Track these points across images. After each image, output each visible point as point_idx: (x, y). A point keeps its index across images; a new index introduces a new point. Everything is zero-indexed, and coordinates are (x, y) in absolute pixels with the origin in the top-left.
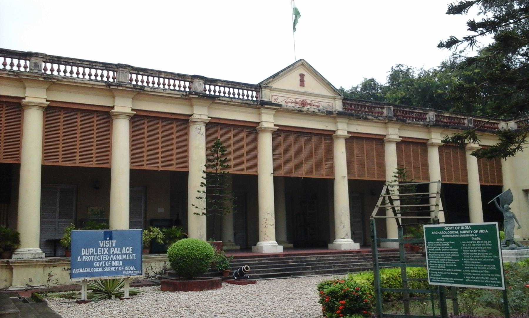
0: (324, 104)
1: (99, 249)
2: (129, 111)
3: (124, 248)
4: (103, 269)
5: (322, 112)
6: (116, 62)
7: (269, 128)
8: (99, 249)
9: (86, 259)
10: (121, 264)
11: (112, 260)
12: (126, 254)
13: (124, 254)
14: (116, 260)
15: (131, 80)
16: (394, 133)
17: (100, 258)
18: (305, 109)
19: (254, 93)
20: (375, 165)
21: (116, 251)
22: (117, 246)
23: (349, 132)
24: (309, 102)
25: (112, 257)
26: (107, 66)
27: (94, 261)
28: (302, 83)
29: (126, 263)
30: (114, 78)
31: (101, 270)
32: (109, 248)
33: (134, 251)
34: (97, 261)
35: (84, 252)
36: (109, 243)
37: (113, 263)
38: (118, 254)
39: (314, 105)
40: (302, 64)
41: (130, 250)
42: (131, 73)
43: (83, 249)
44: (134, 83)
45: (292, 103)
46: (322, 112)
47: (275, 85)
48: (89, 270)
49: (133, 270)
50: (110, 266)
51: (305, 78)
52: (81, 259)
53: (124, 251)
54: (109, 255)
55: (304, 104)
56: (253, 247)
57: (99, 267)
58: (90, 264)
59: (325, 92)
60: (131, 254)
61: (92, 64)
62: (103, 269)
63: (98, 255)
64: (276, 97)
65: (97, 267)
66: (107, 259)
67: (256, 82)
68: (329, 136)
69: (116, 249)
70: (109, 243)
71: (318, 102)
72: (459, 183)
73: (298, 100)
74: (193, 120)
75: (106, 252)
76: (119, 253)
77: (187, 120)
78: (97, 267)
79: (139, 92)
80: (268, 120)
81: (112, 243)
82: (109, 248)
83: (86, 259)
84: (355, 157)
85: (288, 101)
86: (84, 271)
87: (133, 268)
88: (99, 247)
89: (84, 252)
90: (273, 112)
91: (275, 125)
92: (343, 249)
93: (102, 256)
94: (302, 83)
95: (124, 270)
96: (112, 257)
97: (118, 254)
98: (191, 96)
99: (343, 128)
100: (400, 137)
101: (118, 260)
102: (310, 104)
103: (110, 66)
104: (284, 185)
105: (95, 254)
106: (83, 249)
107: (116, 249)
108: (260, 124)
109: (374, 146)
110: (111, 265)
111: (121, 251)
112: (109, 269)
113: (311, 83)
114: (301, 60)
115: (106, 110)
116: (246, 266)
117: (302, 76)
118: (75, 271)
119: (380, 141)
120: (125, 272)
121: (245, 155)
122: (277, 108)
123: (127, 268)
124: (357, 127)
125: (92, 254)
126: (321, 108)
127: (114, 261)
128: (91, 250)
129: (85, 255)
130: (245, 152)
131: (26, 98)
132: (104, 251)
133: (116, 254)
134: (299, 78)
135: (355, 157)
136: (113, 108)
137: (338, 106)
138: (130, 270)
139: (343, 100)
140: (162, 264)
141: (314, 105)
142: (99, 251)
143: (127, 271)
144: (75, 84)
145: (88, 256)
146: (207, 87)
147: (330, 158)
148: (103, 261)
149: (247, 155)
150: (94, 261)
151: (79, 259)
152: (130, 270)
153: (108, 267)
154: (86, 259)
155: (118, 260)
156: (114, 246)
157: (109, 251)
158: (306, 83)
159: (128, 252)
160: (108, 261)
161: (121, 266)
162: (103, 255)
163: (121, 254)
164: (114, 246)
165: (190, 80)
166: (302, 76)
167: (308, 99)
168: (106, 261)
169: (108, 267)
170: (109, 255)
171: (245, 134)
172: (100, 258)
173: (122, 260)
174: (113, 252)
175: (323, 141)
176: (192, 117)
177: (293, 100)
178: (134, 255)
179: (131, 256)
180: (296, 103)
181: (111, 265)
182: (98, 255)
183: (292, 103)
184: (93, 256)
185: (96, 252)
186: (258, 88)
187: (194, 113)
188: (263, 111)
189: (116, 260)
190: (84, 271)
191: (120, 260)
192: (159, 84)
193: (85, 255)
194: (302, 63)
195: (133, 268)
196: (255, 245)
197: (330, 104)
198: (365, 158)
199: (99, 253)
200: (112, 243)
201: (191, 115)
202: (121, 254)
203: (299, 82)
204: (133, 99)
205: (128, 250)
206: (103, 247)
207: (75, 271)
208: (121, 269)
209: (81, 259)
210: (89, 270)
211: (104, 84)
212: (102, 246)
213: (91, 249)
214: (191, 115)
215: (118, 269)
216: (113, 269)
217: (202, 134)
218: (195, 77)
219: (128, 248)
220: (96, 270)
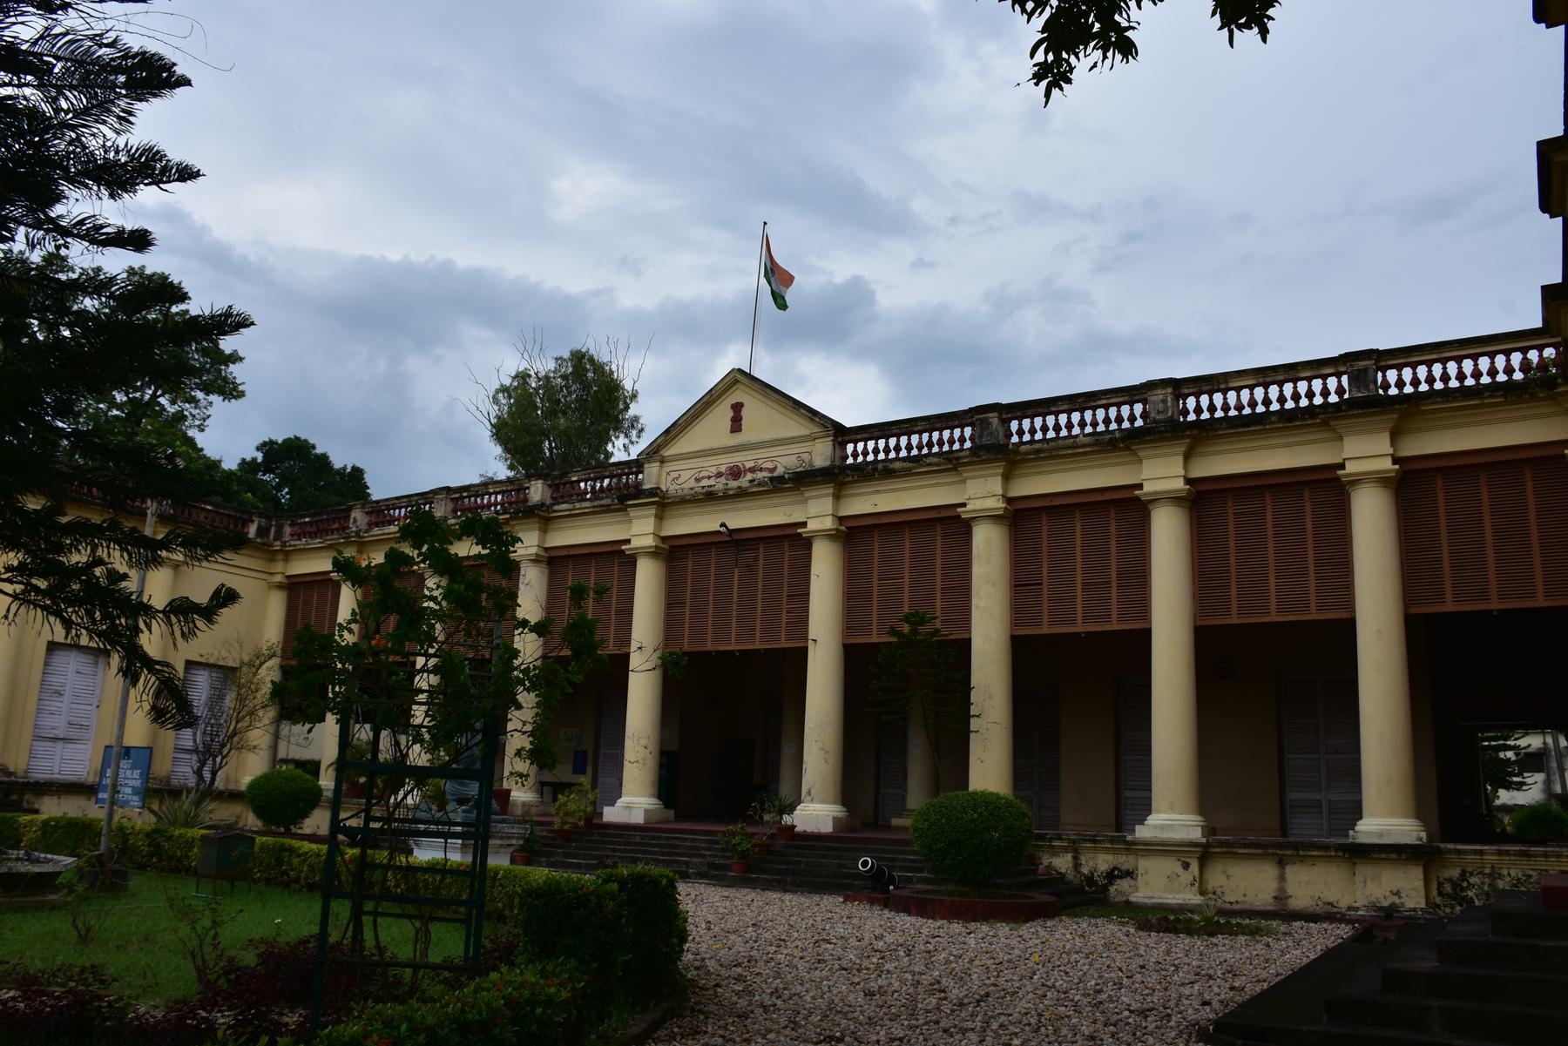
0: (786, 461)
5: (759, 485)
18: (744, 481)
20: (938, 596)
24: (749, 465)
40: (737, 381)
46: (759, 485)
47: (667, 452)
51: (745, 413)
55: (736, 473)
72: (1307, 617)
73: (723, 469)
84: (876, 582)
90: (652, 511)
99: (816, 512)
102: (752, 470)
109: (939, 539)
113: (761, 421)
117: (737, 408)
122: (664, 504)
124: (876, 498)
126: (779, 471)
131: (1347, 464)
134: (731, 414)
135: (876, 582)
139: (835, 435)
141: (761, 470)
147: (802, 595)
149: (617, 612)
166: (737, 408)
167: (746, 459)
180: (719, 475)
188: (633, 513)
197: (806, 457)
198: (907, 580)
203: (729, 424)
211: (936, 460)
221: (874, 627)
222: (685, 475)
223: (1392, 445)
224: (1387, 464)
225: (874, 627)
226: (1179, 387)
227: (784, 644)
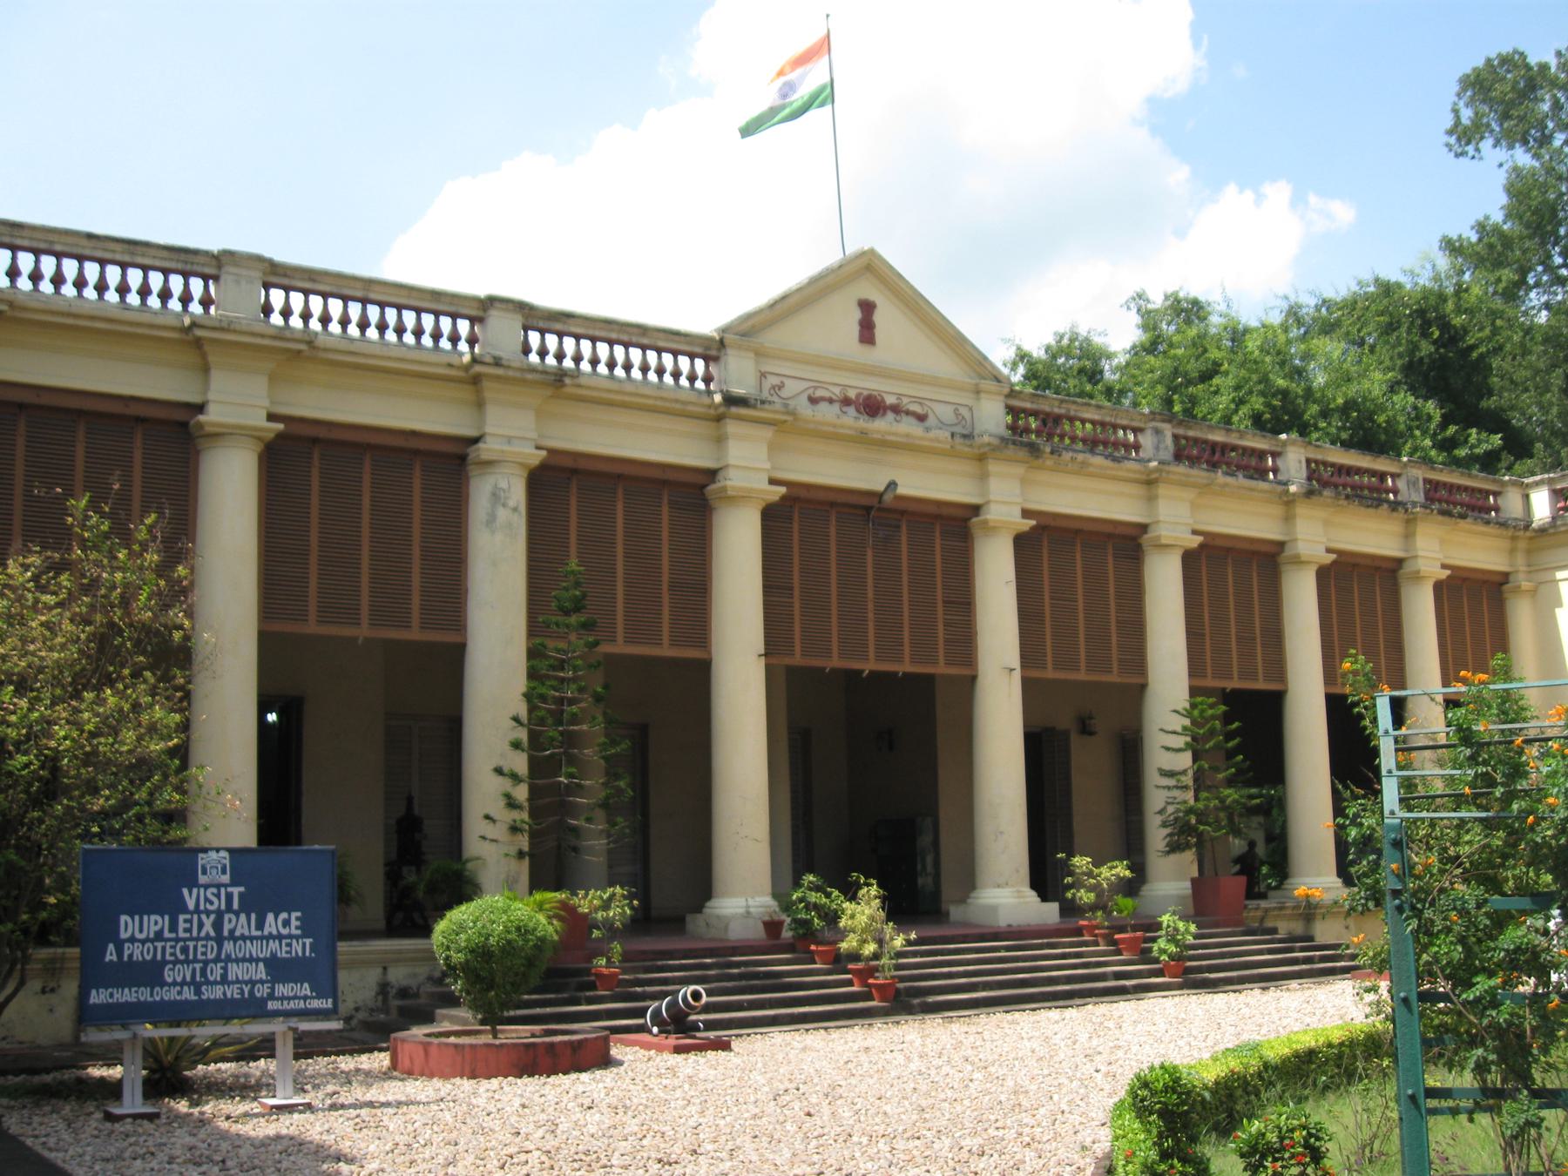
1: (182, 917)
2: (259, 420)
3: (270, 917)
4: (198, 992)
6: (214, 246)
7: (751, 490)
8: (182, 917)
9: (136, 952)
10: (261, 972)
11: (229, 959)
12: (280, 937)
13: (270, 937)
14: (244, 960)
15: (267, 310)
16: (1181, 515)
17: (185, 950)
19: (700, 365)
21: (242, 924)
22: (247, 906)
23: (1026, 513)
24: (890, 400)
25: (228, 947)
26: (183, 260)
27: (164, 962)
28: (867, 333)
29: (280, 969)
30: (206, 302)
31: (188, 994)
32: (220, 914)
33: (307, 929)
34: (175, 963)
35: (127, 925)
36: (218, 896)
37: (235, 971)
38: (252, 938)
39: (908, 413)
41: (294, 923)
42: (267, 286)
43: (124, 918)
44: (276, 319)
45: (831, 401)
48: (144, 994)
49: (305, 998)
50: (224, 980)
51: (879, 318)
52: (120, 952)
53: (272, 924)
54: (220, 940)
55: (872, 407)
56: (689, 918)
57: (183, 983)
58: (151, 973)
59: (944, 365)
60: (297, 938)
61: (129, 252)
62: (198, 992)
63: (177, 940)
64: (775, 381)
65: (175, 983)
66: (211, 956)
67: (705, 322)
68: (956, 526)
69: (243, 917)
70: (218, 896)
71: (920, 401)
73: (852, 394)
74: (485, 456)
75: (208, 928)
76: (255, 933)
77: (462, 459)
78: (175, 983)
79: (297, 354)
80: (750, 467)
81: (229, 897)
82: (220, 914)
83: (137, 956)
85: (819, 393)
86: (126, 995)
87: (306, 989)
88: (185, 910)
89: (127, 925)
91: (773, 482)
92: (1003, 921)
93: (191, 944)
94: (867, 333)
95: (271, 996)
96: (228, 947)
97: (252, 938)
98: (478, 368)
100: (1195, 532)
101: (251, 960)
102: (896, 409)
103: (190, 258)
104: (799, 701)
105: (167, 934)
106: (124, 918)
107: (243, 917)
108: (720, 476)
110: (224, 976)
111: (260, 926)
112: (217, 992)
114: (863, 254)
115: (179, 416)
116: (692, 987)
117: (867, 308)
118: (98, 997)
119: (1127, 545)
120: (271, 1005)
121: (665, 586)
123: (282, 989)
125: (159, 936)
127: (237, 961)
128: (155, 922)
129: (132, 940)
130: (665, 578)
132: (201, 925)
133: (243, 938)
134: (857, 314)
136: (200, 408)
137: (992, 417)
138: (295, 997)
140: (373, 976)
141: (908, 413)
142: (182, 925)
143: (282, 998)
144: (70, 321)
145: (143, 942)
146: (534, 338)
147: (962, 603)
148: (196, 960)
149: (672, 587)
150: (164, 962)
151: (111, 955)
152: (295, 997)
153: (216, 983)
154: (137, 953)
155: (251, 960)
156: (236, 906)
157: (218, 925)
158: (879, 333)
159: (285, 932)
160: (217, 960)
161: (262, 982)
162: (198, 939)
163: (262, 938)
164: (236, 906)
165: (473, 313)
166: (867, 308)
168: (206, 963)
169: (216, 983)
170: (220, 940)
171: (665, 510)
172: (185, 950)
173: (265, 960)
174: (232, 932)
175: (938, 542)
176: (481, 445)
177: (837, 390)
178: (308, 941)
179: (297, 948)
181: (224, 976)
182: (177, 940)
183: (831, 401)
184: (159, 945)
185: (174, 927)
186: (711, 350)
187: (732, 461)
189: (244, 960)
190: (126, 995)
191: (257, 960)
192: (363, 325)
193: (132, 940)
194: (868, 266)
195: (306, 989)
196: (699, 908)
197: (964, 412)
199: (182, 934)
200: (229, 897)
201: (476, 441)
202: (262, 938)
203: (855, 330)
204: (273, 379)
205: (286, 923)
206: (197, 911)
207: (98, 997)
208: (262, 991)
209: (120, 952)
210: (144, 994)
212: (191, 905)
213: (153, 917)
214: (476, 441)
215: (251, 992)
216: (233, 992)
217: (515, 510)
218: (491, 302)
219: (284, 915)
220: (171, 994)
221: (1049, 659)
222: (791, 388)
223: (770, 458)
224: (261, 422)
225: (1049, 659)
226: (534, 318)
227: (906, 667)
